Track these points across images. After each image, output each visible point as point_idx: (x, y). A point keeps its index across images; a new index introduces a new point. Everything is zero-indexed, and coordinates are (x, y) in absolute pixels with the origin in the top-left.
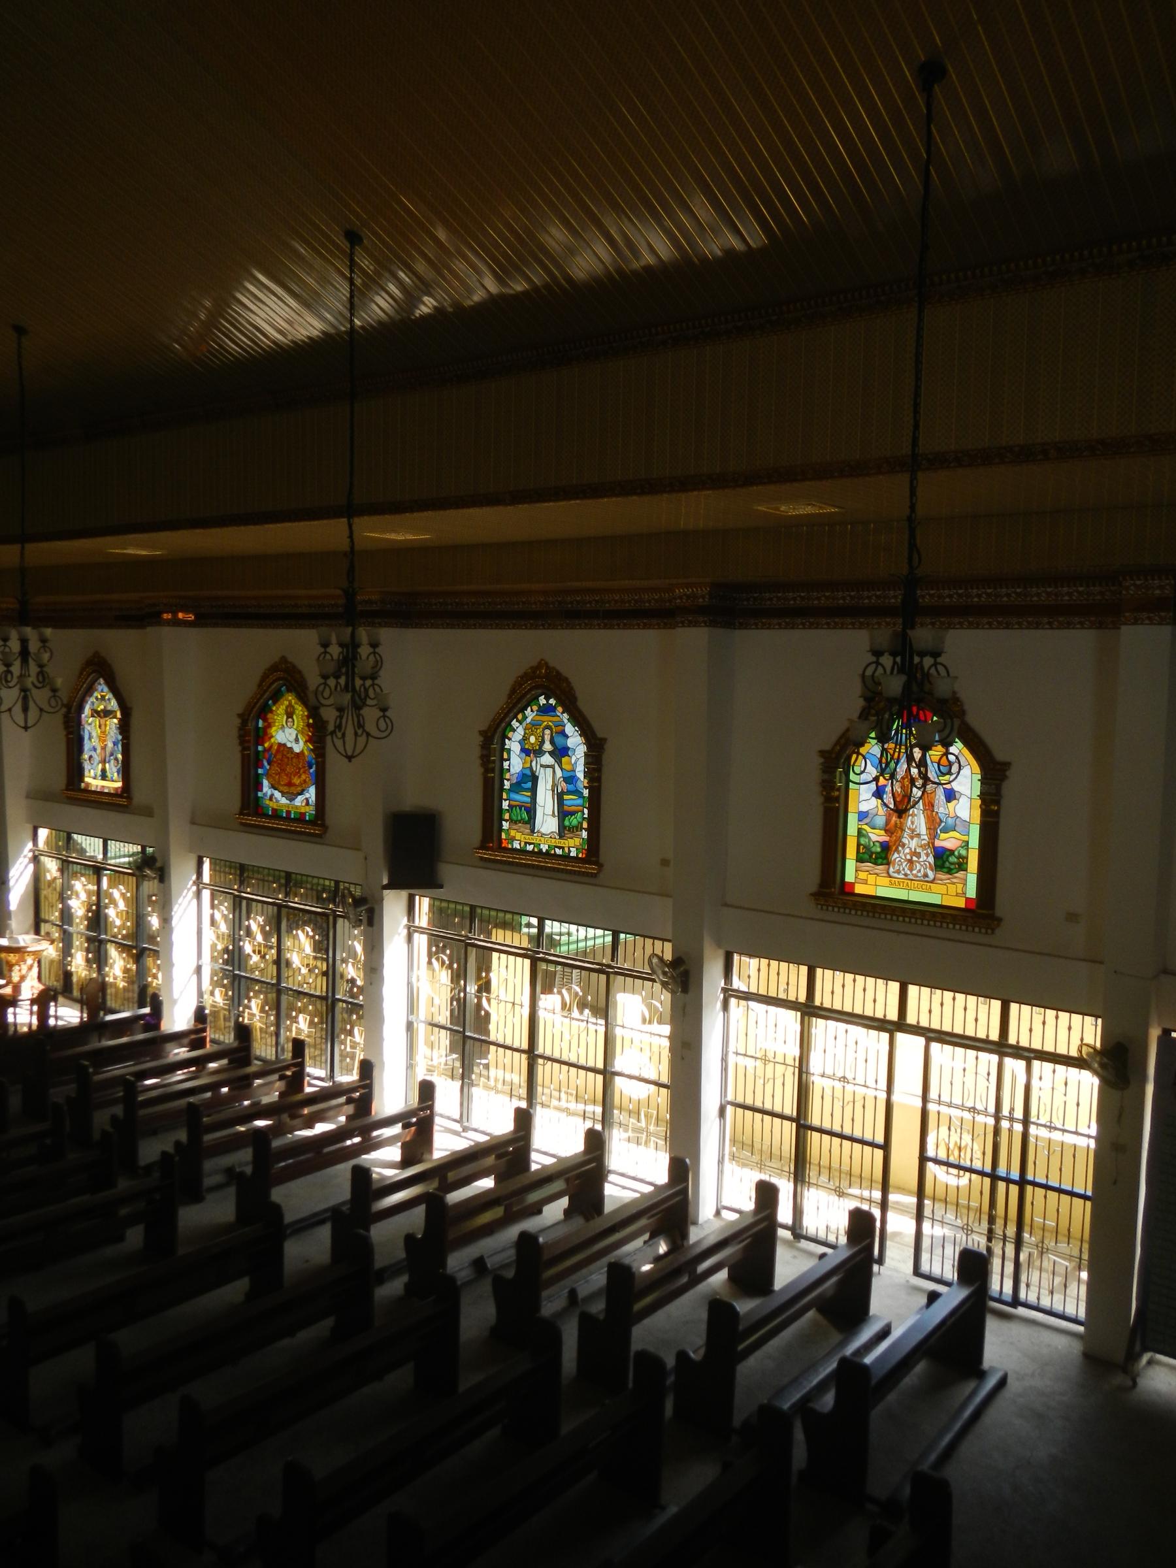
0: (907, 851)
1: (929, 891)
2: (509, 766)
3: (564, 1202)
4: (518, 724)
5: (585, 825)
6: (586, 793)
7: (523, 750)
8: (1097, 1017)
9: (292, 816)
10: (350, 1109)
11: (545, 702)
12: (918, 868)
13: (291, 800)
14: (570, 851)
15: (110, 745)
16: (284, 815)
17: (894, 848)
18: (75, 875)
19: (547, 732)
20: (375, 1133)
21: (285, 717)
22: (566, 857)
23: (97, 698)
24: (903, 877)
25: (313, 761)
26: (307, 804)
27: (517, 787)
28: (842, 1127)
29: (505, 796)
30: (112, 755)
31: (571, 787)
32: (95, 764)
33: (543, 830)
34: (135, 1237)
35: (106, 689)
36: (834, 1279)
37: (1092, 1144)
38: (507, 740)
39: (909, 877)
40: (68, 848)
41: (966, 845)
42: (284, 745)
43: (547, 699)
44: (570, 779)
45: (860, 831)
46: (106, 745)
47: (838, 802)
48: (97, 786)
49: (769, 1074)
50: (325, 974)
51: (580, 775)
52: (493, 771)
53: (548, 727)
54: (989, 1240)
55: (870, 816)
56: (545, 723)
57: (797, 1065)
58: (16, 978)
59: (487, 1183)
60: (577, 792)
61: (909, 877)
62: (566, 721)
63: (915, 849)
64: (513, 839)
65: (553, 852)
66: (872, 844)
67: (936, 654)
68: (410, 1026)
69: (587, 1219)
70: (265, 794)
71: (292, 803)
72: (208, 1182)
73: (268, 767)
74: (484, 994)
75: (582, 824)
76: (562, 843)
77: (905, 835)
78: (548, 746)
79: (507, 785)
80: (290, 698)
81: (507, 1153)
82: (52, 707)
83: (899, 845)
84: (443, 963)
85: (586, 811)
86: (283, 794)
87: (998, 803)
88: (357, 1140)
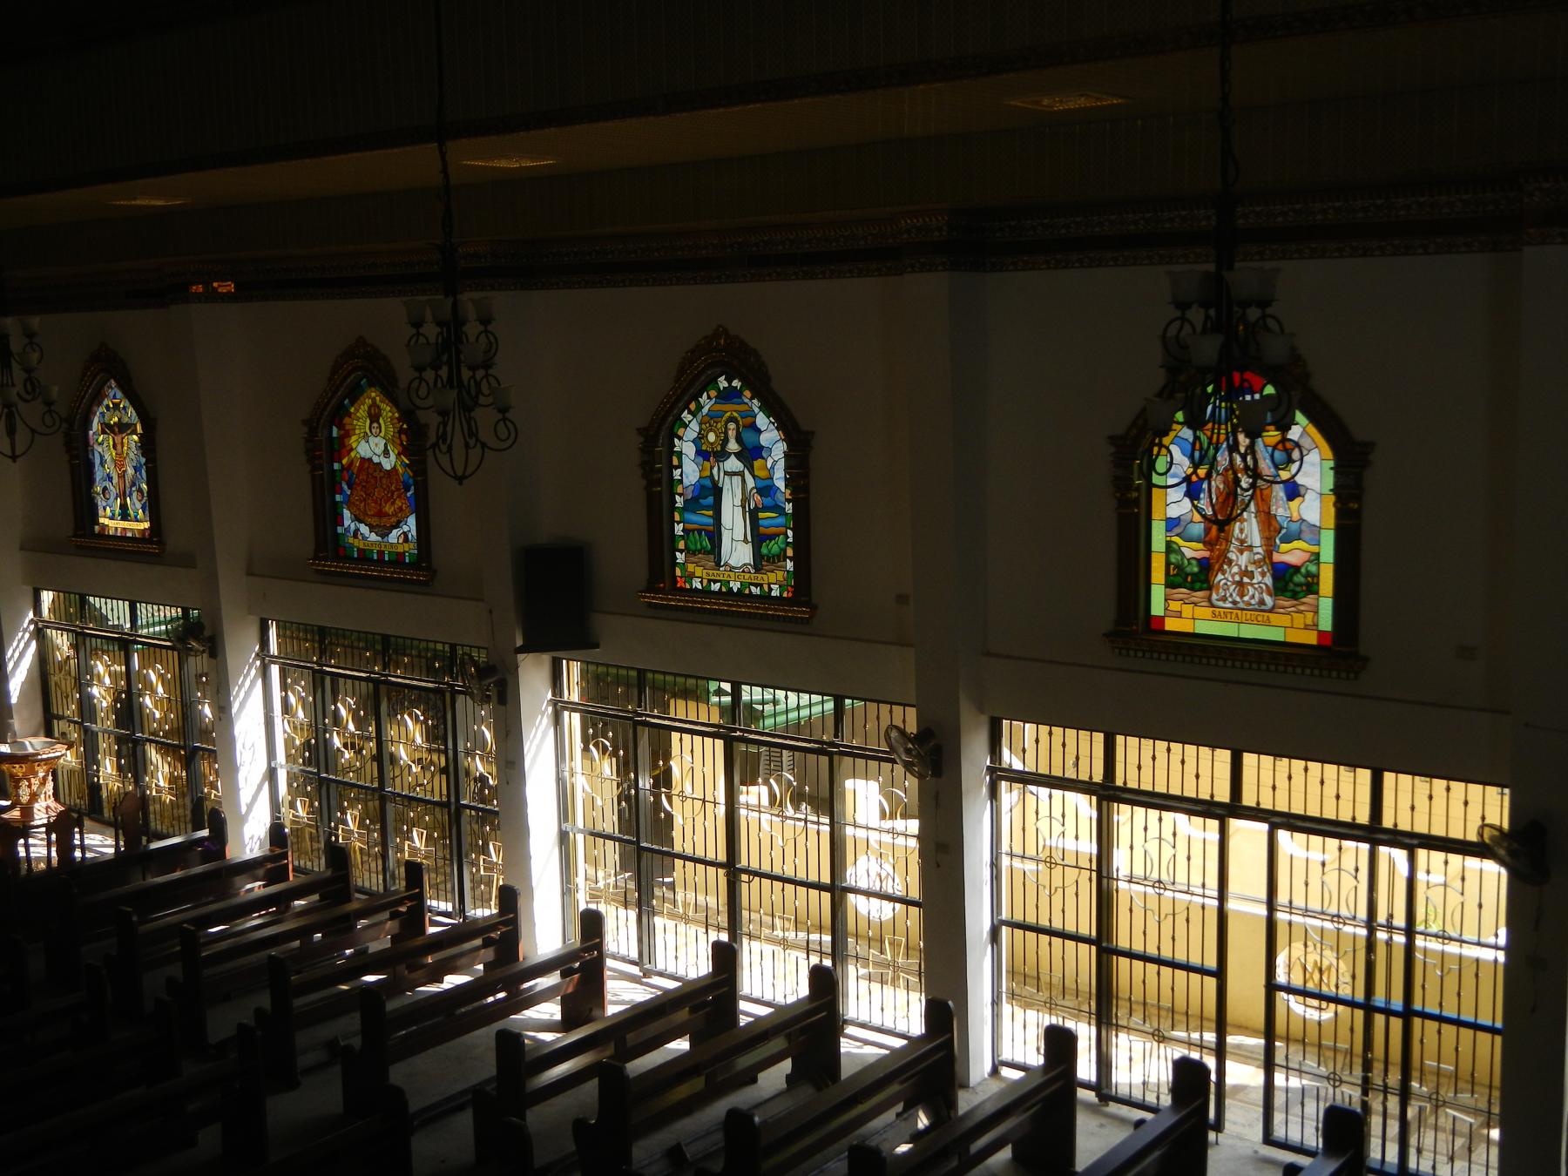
0: (1235, 569)
1: (1268, 623)
2: (681, 475)
3: (786, 1066)
4: (690, 417)
5: (790, 552)
6: (789, 508)
7: (699, 452)
8: (1503, 786)
9: (387, 559)
10: (489, 954)
11: (726, 385)
12: (1251, 593)
13: (384, 535)
14: (771, 590)
15: (130, 471)
16: (375, 557)
17: (1217, 567)
18: (95, 653)
19: (732, 426)
20: (526, 985)
21: (368, 421)
22: (766, 598)
23: (108, 407)
24: (1230, 605)
25: (411, 481)
26: (406, 540)
27: (693, 504)
28: (1159, 949)
29: (677, 517)
30: (133, 484)
31: (768, 501)
32: (112, 498)
33: (732, 562)
34: (210, 1139)
35: (119, 394)
36: (1156, 1154)
37: (1501, 957)
38: (676, 440)
39: (1239, 605)
40: (82, 617)
41: (1316, 558)
42: (370, 460)
43: (729, 381)
44: (766, 489)
45: (1169, 544)
46: (125, 472)
47: (1138, 507)
48: (116, 528)
49: (1057, 882)
50: (444, 771)
51: (780, 484)
52: (659, 482)
53: (732, 419)
54: (1365, 1093)
55: (1183, 523)
56: (728, 414)
57: (1094, 867)
58: (25, 799)
59: (682, 1045)
60: (778, 509)
61: (1239, 605)
62: (756, 410)
63: (1246, 567)
64: (692, 576)
65: (747, 592)
66: (1186, 562)
67: (1264, 304)
68: (563, 838)
69: (819, 1089)
70: (347, 530)
71: (385, 540)
72: (304, 1061)
74: (663, 790)
75: (785, 551)
77: (1232, 549)
78: (733, 446)
79: (679, 501)
80: (373, 394)
81: (706, 1004)
82: (47, 426)
83: (1224, 562)
84: (605, 749)
85: (790, 533)
87: (1358, 499)
88: (501, 995)
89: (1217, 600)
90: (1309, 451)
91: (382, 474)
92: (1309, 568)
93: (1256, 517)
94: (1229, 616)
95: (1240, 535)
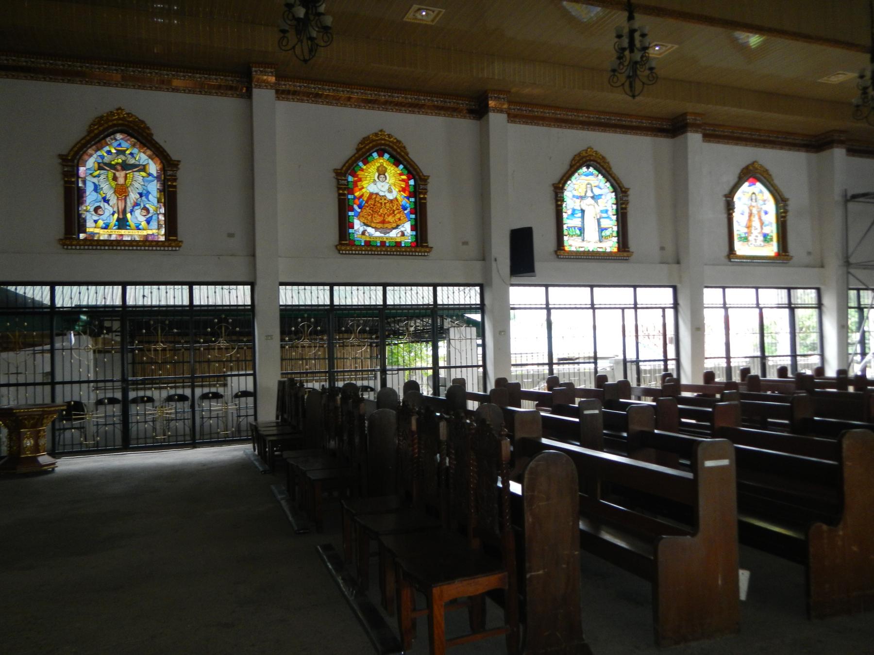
5: (615, 234)
21: (377, 174)
30: (136, 204)
31: (604, 215)
33: (589, 240)
41: (772, 232)
42: (377, 194)
43: (588, 168)
73: (359, 210)
75: (612, 234)
76: (600, 245)
78: (589, 194)
79: (565, 215)
86: (376, 229)
91: (386, 201)
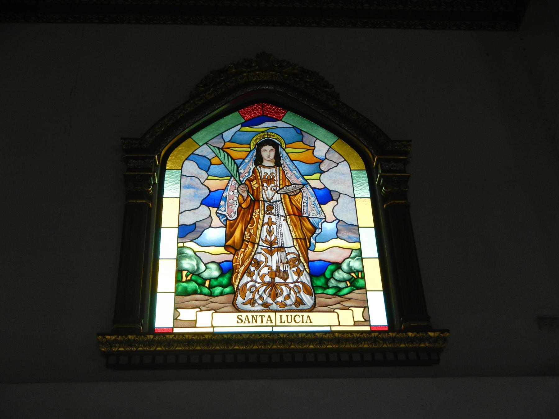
0: (265, 270)
12: (285, 293)
17: (242, 269)
24: (261, 308)
45: (180, 255)
63: (278, 267)
77: (259, 250)
89: (242, 303)
90: (338, 164)
92: (351, 264)
93: (286, 220)
94: (259, 320)
95: (268, 237)
